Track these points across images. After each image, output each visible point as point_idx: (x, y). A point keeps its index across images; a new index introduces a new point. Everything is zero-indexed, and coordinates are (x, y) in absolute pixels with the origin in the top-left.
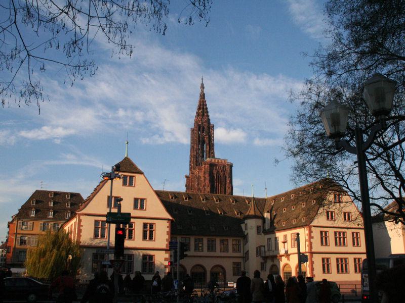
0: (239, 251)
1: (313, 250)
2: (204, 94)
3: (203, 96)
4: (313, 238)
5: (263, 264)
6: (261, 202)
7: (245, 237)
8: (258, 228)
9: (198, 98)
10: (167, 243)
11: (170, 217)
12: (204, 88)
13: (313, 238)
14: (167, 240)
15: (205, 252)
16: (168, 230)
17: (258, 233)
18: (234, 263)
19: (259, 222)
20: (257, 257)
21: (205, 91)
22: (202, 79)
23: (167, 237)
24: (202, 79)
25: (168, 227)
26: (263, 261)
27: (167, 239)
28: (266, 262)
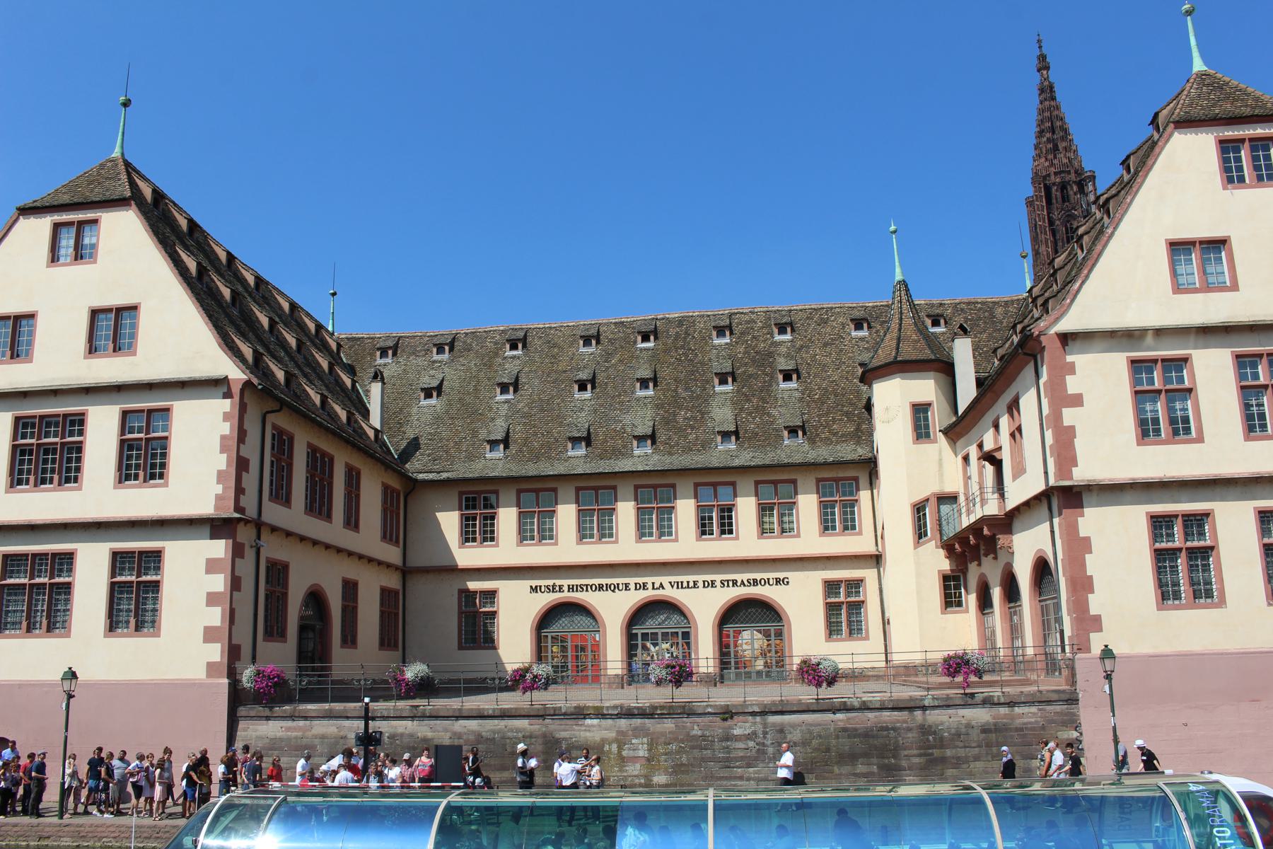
0: (850, 526)
1: (1082, 474)
2: (1051, 87)
3: (1047, 91)
4: (1077, 401)
5: (956, 578)
6: (999, 311)
7: (870, 467)
8: (920, 411)
9: (1034, 100)
10: (219, 489)
11: (236, 374)
12: (1047, 68)
13: (1077, 401)
14: (221, 476)
15: (686, 542)
16: (227, 432)
17: (921, 432)
18: (831, 587)
19: (925, 388)
20: (915, 548)
21: (1053, 76)
22: (1039, 41)
23: (221, 462)
24: (1039, 41)
25: (226, 417)
26: (946, 565)
27: (220, 473)
28: (965, 572)
